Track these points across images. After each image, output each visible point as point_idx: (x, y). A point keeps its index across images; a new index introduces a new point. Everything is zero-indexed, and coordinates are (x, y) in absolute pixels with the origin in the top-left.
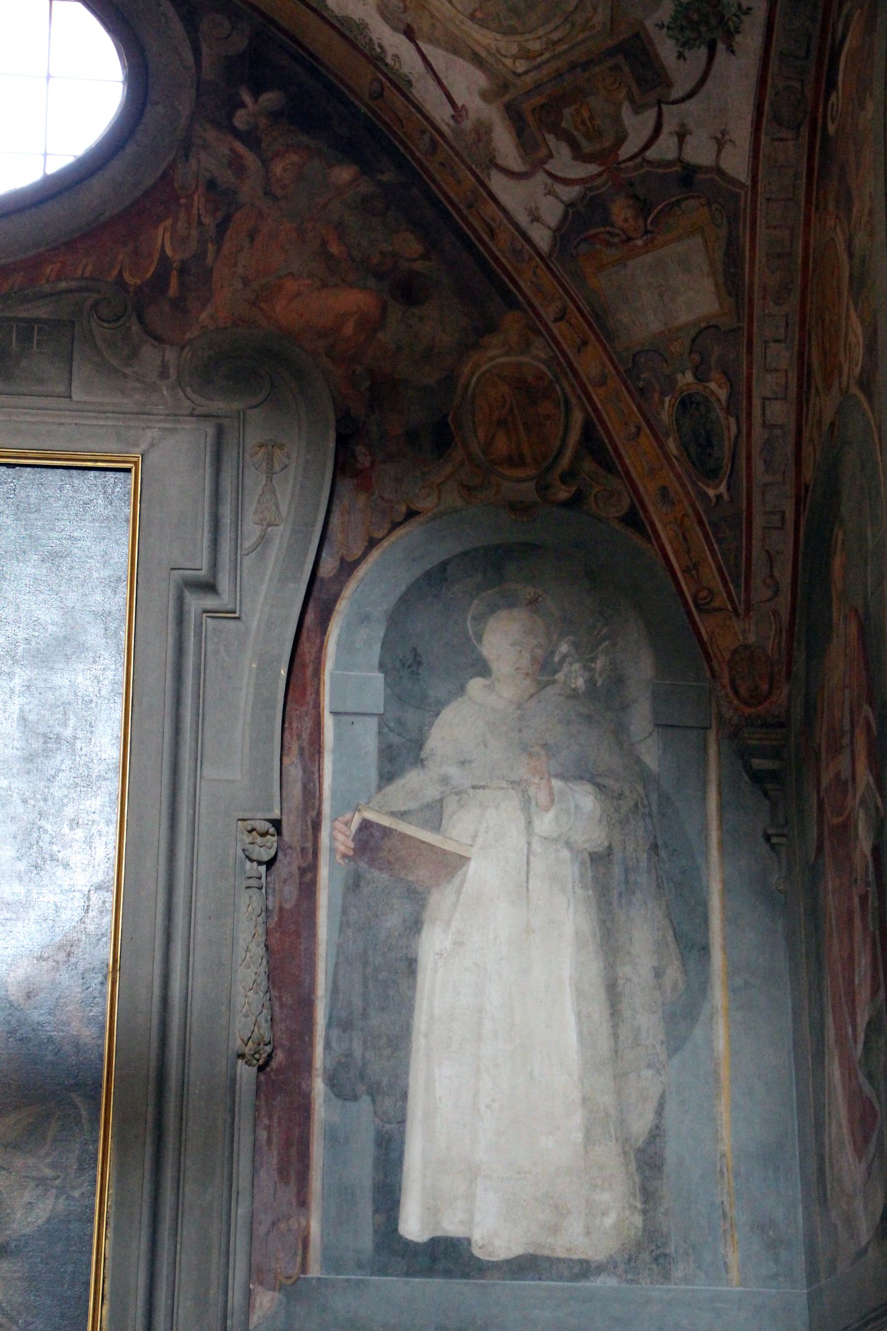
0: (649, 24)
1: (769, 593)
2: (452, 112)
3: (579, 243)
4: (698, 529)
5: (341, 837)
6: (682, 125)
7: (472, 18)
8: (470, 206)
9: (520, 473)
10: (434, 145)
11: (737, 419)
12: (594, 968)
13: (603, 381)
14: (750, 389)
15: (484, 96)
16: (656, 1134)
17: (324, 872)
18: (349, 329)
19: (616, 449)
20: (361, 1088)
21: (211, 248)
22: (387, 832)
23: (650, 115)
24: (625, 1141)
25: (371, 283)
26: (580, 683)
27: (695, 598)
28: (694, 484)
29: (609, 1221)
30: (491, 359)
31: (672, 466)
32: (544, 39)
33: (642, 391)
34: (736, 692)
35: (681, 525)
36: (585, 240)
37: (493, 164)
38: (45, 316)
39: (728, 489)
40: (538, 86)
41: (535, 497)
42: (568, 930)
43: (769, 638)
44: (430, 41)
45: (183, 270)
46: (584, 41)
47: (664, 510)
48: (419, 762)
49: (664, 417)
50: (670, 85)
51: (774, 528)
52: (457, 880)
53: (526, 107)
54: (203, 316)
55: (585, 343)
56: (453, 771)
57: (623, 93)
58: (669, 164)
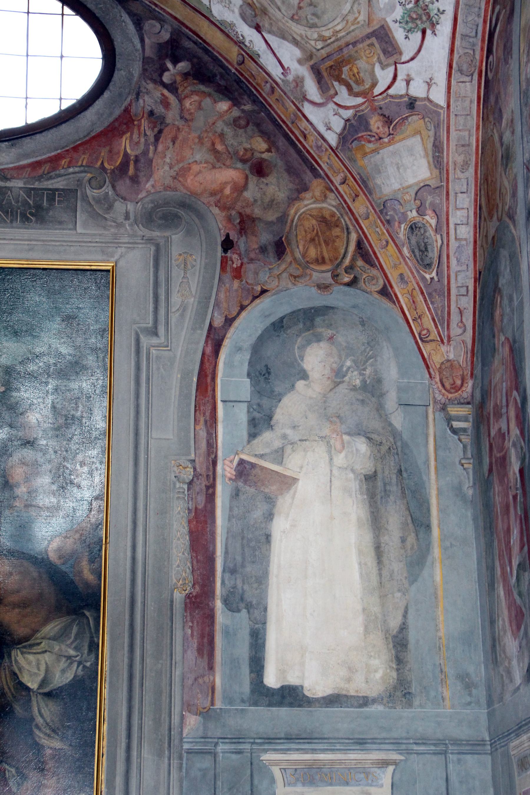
0: (389, 20)
1: (460, 331)
2: (282, 71)
3: (352, 142)
4: (421, 296)
5: (228, 469)
6: (408, 75)
7: (292, 18)
8: (293, 123)
9: (324, 268)
10: (273, 90)
11: (441, 235)
12: (368, 537)
14: (448, 220)
15: (300, 62)
16: (403, 627)
17: (219, 488)
18: (227, 191)
19: (375, 253)
20: (242, 605)
21: (152, 148)
22: (253, 466)
24: (387, 631)
25: (239, 165)
26: (358, 382)
27: (420, 334)
28: (418, 272)
30: (306, 206)
31: (406, 264)
32: (332, 30)
33: (388, 222)
34: (443, 385)
35: (412, 296)
36: (355, 139)
37: (305, 98)
38: (62, 187)
39: (437, 275)
40: (329, 56)
41: (330, 281)
42: (354, 517)
43: (460, 356)
44: (269, 32)
45: (137, 160)
46: (353, 31)
47: (402, 286)
48: (271, 427)
49: (401, 236)
50: (401, 53)
51: (463, 295)
52: (292, 492)
53: (323, 67)
54: (148, 185)
55: (357, 196)
56: (289, 432)
57: (375, 59)
58: (401, 96)
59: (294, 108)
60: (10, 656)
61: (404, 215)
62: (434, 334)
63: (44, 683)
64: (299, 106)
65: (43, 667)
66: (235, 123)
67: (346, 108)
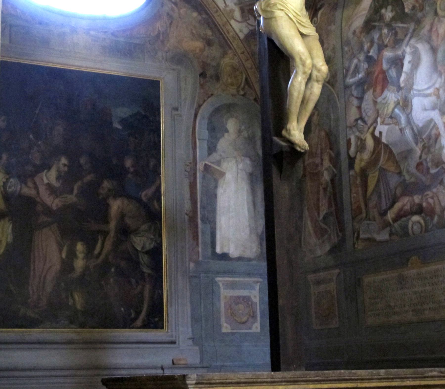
5: (201, 167)
9: (233, 88)
10: (217, 11)
12: (251, 198)
17: (198, 175)
18: (198, 51)
20: (207, 222)
22: (210, 166)
24: (257, 234)
29: (255, 250)
37: (233, 18)
42: (245, 189)
52: (223, 178)
56: (223, 154)
60: (130, 237)
63: (143, 248)
65: (142, 242)
67: (252, 25)
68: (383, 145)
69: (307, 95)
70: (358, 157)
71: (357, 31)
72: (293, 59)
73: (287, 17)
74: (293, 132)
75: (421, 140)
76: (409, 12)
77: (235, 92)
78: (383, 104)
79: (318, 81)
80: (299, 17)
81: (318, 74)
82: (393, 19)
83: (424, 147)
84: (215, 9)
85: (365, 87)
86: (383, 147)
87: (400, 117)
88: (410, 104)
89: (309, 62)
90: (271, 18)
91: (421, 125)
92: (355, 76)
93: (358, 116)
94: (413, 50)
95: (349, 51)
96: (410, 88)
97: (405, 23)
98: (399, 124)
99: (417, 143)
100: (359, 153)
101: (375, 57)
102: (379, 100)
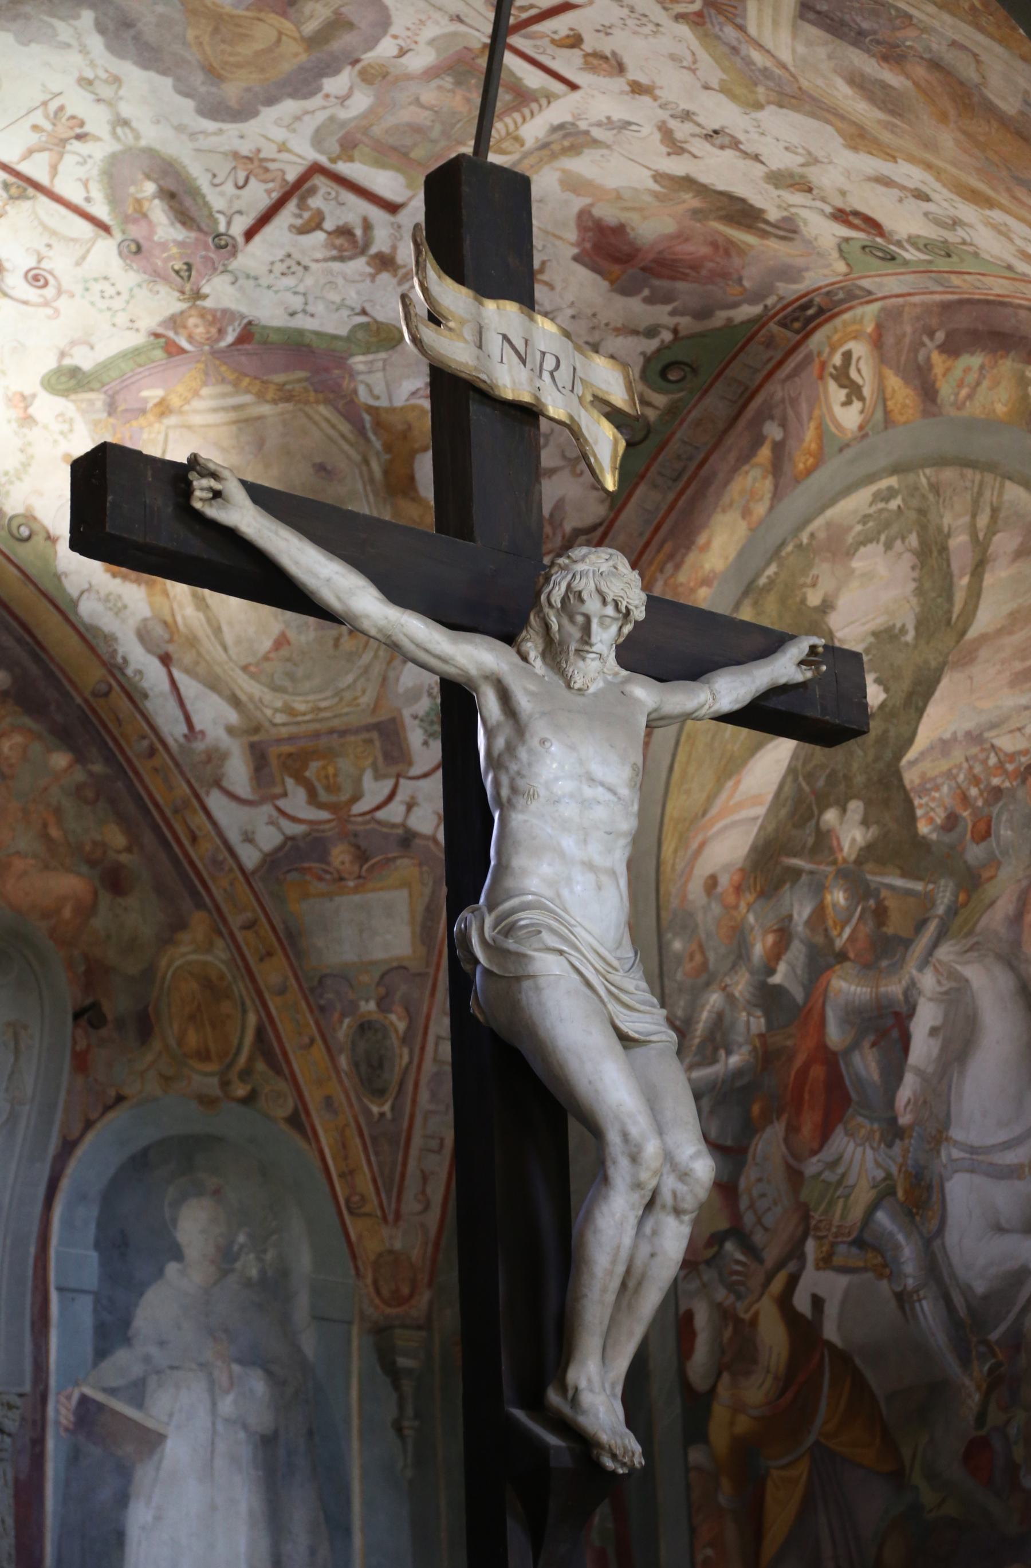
0: (407, 713)
1: (418, 1207)
3: (289, 871)
5: (63, 1411)
6: (413, 798)
7: (245, 669)
8: (176, 811)
10: (152, 752)
12: (264, 1545)
13: (282, 991)
15: (230, 730)
17: (50, 1444)
18: (67, 913)
19: (285, 1054)
22: (101, 1407)
23: (387, 786)
25: (84, 869)
26: (254, 1272)
27: (348, 1201)
30: (184, 955)
31: (341, 1081)
32: (310, 705)
33: (322, 1009)
34: (378, 1291)
36: (296, 869)
37: (217, 783)
40: (291, 739)
41: (217, 1092)
42: (243, 1508)
44: (187, 671)
46: (347, 714)
50: (410, 764)
52: (156, 1457)
53: (273, 751)
55: (270, 954)
56: (154, 1350)
57: (370, 761)
58: (394, 826)
59: (188, 791)
61: (354, 1005)
62: (372, 1205)
64: (202, 792)
66: (78, 791)
68: (826, 1353)
69: (639, 1263)
70: (723, 1391)
71: (725, 882)
72: (595, 1131)
73: (575, 977)
74: (587, 1399)
75: (982, 1349)
76: (934, 836)
77: (212, 1085)
78: (828, 1184)
79: (677, 1212)
80: (615, 977)
81: (681, 1188)
82: (868, 853)
83: (994, 1382)
84: (145, 743)
85: (756, 1109)
86: (827, 1359)
87: (898, 1247)
88: (935, 1198)
89: (651, 1148)
90: (518, 979)
91: (980, 1287)
92: (714, 1061)
93: (723, 1225)
94: (947, 985)
95: (692, 957)
96: (939, 1138)
97: (918, 878)
98: (891, 1273)
99: (965, 1361)
100: (726, 1377)
101: (798, 993)
102: (812, 1166)
